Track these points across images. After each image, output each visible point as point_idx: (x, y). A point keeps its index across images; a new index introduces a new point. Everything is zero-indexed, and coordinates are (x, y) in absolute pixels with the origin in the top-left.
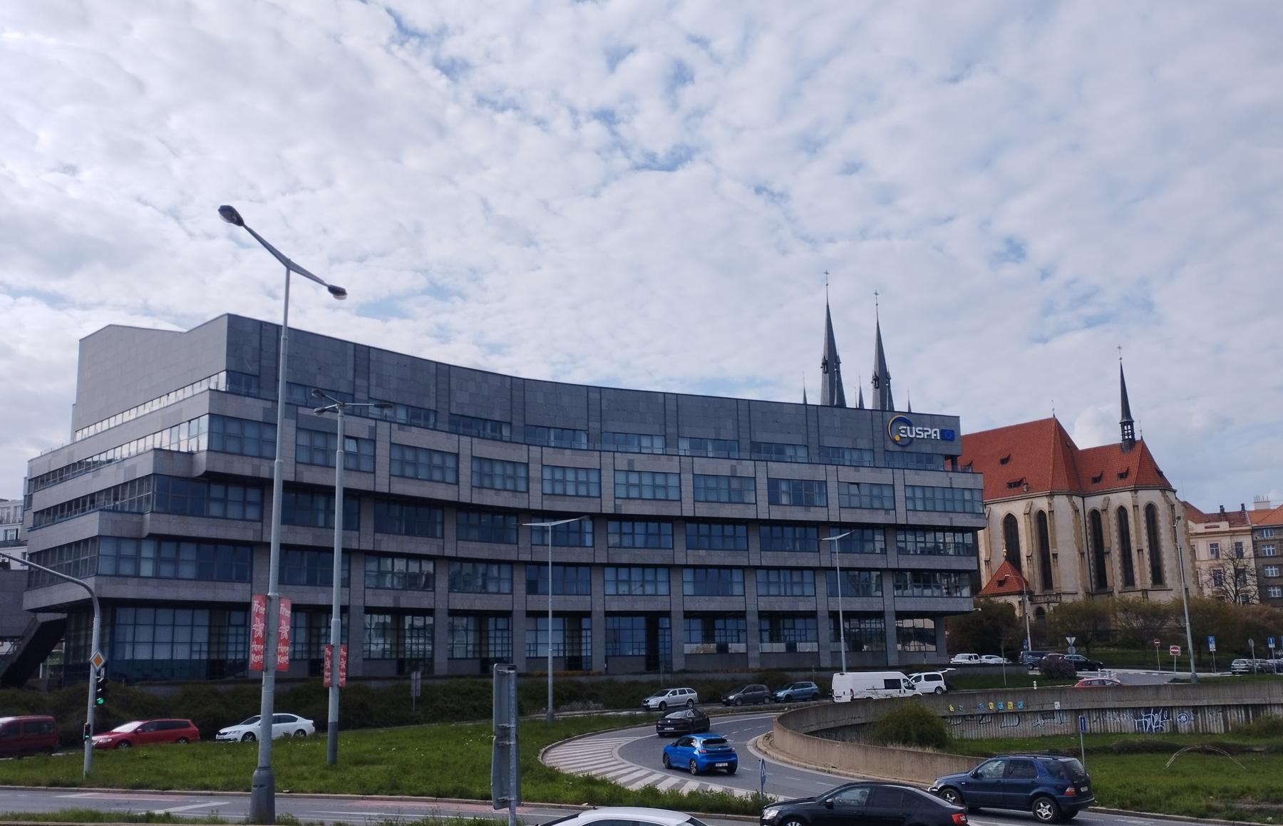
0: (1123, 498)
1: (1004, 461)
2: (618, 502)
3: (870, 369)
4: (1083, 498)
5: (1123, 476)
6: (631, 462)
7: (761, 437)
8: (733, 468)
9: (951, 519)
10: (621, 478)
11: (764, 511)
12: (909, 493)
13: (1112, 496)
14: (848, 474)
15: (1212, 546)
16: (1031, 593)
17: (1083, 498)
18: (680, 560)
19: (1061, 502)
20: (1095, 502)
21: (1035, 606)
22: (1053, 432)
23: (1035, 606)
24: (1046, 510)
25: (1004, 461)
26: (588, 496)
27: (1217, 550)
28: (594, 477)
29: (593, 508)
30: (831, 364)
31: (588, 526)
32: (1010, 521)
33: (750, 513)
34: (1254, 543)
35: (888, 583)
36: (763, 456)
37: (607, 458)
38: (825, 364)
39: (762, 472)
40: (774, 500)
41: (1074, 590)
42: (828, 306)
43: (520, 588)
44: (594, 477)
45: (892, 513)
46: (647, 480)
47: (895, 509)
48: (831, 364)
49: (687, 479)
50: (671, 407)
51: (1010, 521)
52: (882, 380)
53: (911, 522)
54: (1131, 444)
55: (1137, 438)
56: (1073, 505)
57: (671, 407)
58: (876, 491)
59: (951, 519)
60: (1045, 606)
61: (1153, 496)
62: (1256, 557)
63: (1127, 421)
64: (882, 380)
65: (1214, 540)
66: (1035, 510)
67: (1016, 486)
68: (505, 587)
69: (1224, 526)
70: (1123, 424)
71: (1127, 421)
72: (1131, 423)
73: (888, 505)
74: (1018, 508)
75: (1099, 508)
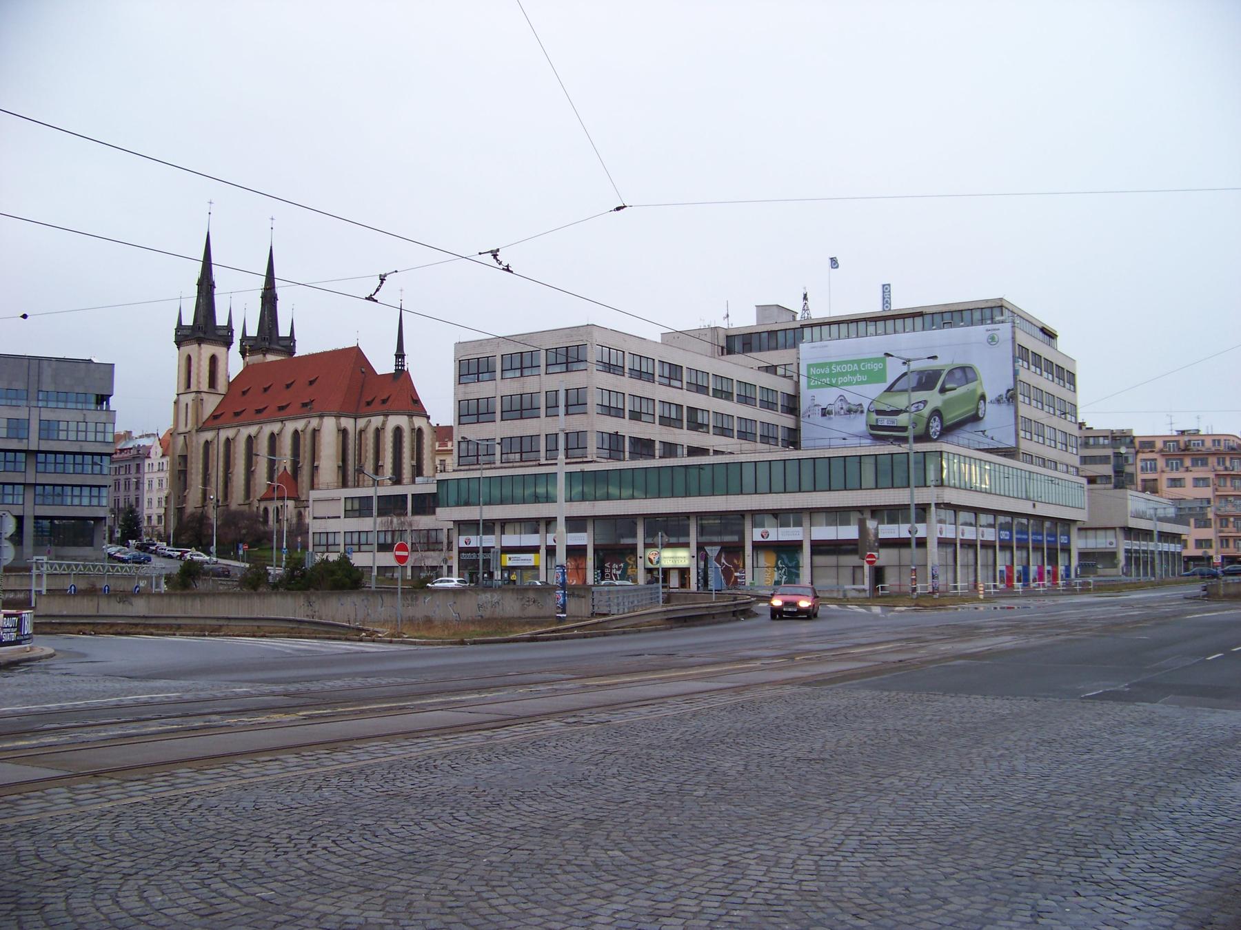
0: (377, 421)
4: (355, 419)
5: (384, 401)
9: (81, 446)
13: (373, 419)
17: (355, 419)
20: (362, 422)
22: (355, 356)
23: (297, 509)
27: (445, 465)
30: (206, 285)
38: (200, 284)
42: (208, 233)
47: (28, 438)
48: (206, 285)
54: (401, 375)
59: (81, 446)
61: (402, 421)
63: (400, 355)
71: (400, 355)
74: (300, 425)
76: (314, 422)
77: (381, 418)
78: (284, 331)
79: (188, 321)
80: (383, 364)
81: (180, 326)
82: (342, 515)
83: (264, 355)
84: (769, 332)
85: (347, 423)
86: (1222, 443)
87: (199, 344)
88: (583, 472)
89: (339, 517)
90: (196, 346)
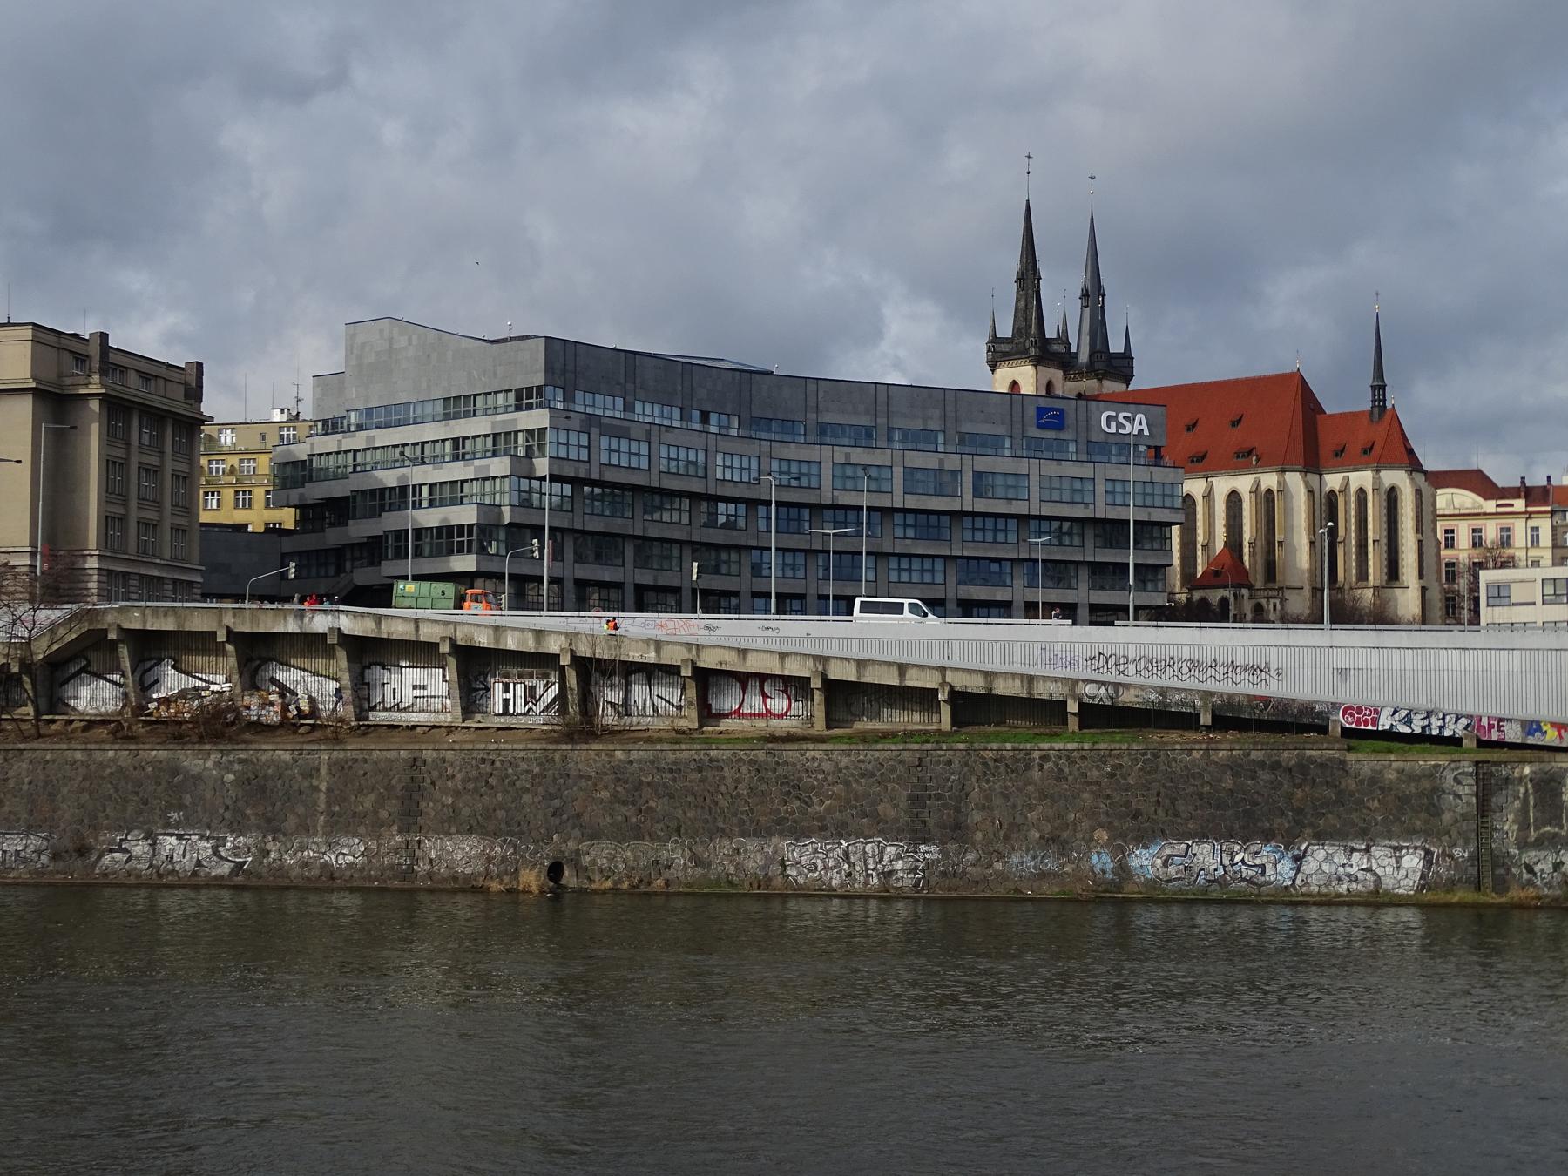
0: (1361, 478)
1: (1235, 423)
2: (836, 493)
3: (1077, 281)
5: (1368, 450)
6: (848, 456)
7: (966, 428)
8: (941, 461)
9: (1149, 514)
11: (967, 503)
12: (1110, 487)
14: (1050, 468)
15: (1502, 530)
16: (1250, 587)
18: (887, 549)
19: (1295, 481)
20: (1333, 481)
21: (1254, 601)
23: (1254, 601)
24: (1275, 488)
25: (1235, 423)
26: (809, 488)
28: (814, 469)
29: (813, 499)
30: (1029, 277)
31: (806, 513)
32: (1234, 498)
33: (954, 505)
34: (1554, 528)
35: (1084, 574)
36: (967, 450)
37: (827, 450)
39: (969, 465)
40: (977, 493)
41: (1299, 585)
43: (747, 571)
44: (814, 469)
45: (1091, 507)
48: (1029, 277)
49: (898, 472)
50: (882, 398)
52: (1093, 295)
53: (1109, 516)
55: (1389, 406)
56: (1306, 483)
57: (882, 398)
58: (1078, 485)
59: (1149, 514)
60: (1264, 601)
61: (1397, 478)
62: (1555, 546)
63: (1379, 389)
64: (1093, 295)
65: (1505, 522)
66: (1264, 487)
67: (1244, 459)
68: (734, 568)
69: (1519, 505)
70: (1374, 388)
71: (1379, 389)
72: (1383, 387)
73: (1089, 499)
74: (1243, 483)
75: (1337, 488)
76: (1270, 480)
78: (1116, 346)
79: (1006, 330)
81: (994, 340)
82: (1539, 600)
83: (1100, 381)
87: (1036, 366)
89: (1534, 604)
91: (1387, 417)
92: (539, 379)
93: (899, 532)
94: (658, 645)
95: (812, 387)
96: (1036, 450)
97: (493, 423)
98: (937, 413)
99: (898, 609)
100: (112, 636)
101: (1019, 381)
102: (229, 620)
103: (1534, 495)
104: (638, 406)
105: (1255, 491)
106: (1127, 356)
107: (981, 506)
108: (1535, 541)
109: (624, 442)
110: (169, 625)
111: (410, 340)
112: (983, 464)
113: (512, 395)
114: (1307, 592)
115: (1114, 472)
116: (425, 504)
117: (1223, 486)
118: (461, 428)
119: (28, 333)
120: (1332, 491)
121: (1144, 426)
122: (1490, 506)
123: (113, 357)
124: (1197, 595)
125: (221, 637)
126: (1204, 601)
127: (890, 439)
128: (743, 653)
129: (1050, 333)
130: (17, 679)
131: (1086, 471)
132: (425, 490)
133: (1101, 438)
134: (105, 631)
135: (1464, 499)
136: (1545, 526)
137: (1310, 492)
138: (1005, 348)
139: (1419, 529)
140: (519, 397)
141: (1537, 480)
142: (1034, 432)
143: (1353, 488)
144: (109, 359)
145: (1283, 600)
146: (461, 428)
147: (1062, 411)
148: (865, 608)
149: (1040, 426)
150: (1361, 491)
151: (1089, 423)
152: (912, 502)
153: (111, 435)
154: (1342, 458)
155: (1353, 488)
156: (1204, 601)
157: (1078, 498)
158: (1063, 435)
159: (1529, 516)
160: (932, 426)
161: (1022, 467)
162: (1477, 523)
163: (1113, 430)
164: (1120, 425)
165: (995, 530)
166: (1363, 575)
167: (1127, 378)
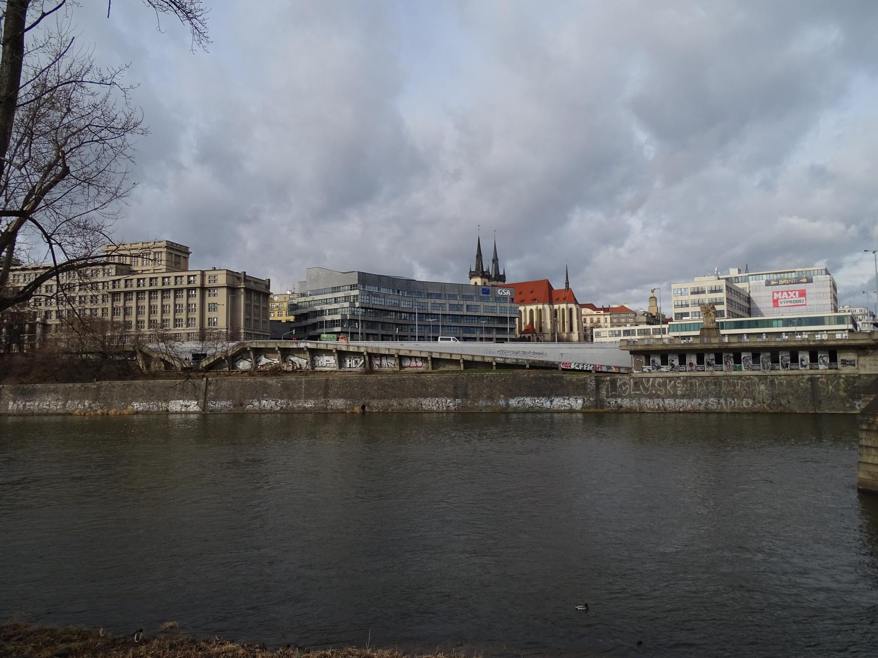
0: (563, 306)
1: (532, 292)
3: (492, 257)
7: (464, 294)
8: (458, 302)
10: (432, 305)
11: (465, 313)
13: (561, 305)
14: (486, 304)
16: (536, 333)
18: (445, 325)
19: (547, 307)
20: (556, 307)
24: (542, 308)
25: (532, 292)
29: (426, 312)
30: (479, 256)
31: (424, 316)
32: (531, 311)
34: (611, 318)
35: (494, 330)
39: (466, 303)
40: (468, 310)
43: (409, 331)
44: (426, 304)
46: (438, 305)
48: (479, 256)
49: (447, 305)
50: (443, 286)
51: (531, 311)
56: (549, 307)
57: (443, 286)
58: (493, 308)
62: (611, 323)
63: (567, 283)
64: (495, 260)
66: (539, 308)
67: (534, 301)
69: (602, 312)
70: (566, 283)
71: (567, 283)
74: (534, 307)
75: (557, 308)
76: (540, 306)
77: (565, 305)
78: (501, 273)
79: (473, 269)
80: (558, 285)
81: (471, 272)
84: (736, 277)
85: (551, 306)
86: (863, 311)
88: (725, 322)
90: (480, 279)
91: (570, 290)
92: (356, 282)
93: (448, 320)
94: (389, 349)
95: (425, 283)
96: (482, 299)
97: (345, 294)
98: (457, 290)
99: (449, 339)
100: (248, 349)
101: (477, 282)
102: (278, 345)
103: (606, 310)
104: (382, 289)
105: (537, 309)
106: (504, 276)
107: (469, 313)
108: (606, 321)
109: (378, 298)
110: (263, 346)
111: (323, 273)
112: (469, 303)
113: (349, 287)
114: (550, 335)
115: (502, 305)
116: (327, 314)
117: (529, 308)
118: (337, 295)
119: (225, 272)
120: (556, 309)
121: (509, 293)
122: (595, 313)
123: (247, 278)
124: (522, 335)
125: (277, 349)
126: (524, 337)
127: (445, 297)
128: (410, 351)
129: (485, 270)
130: (224, 361)
131: (494, 304)
132: (327, 311)
133: (498, 296)
134: (247, 348)
135: (588, 311)
136: (608, 317)
137: (550, 309)
138: (474, 274)
139: (578, 318)
140: (351, 287)
141: (606, 306)
142: (482, 295)
143: (561, 309)
144: (246, 279)
145: (544, 336)
146: (337, 295)
147: (488, 289)
148: (441, 339)
149: (483, 293)
150: (563, 309)
151: (496, 292)
152: (451, 313)
153: (247, 298)
154: (558, 301)
155: (561, 309)
156: (524, 337)
157: (493, 311)
158: (488, 295)
159: (604, 315)
160: (456, 293)
161: (479, 303)
162: (592, 317)
163: (501, 294)
164: (503, 293)
165: (472, 320)
166: (564, 330)
167: (504, 281)
